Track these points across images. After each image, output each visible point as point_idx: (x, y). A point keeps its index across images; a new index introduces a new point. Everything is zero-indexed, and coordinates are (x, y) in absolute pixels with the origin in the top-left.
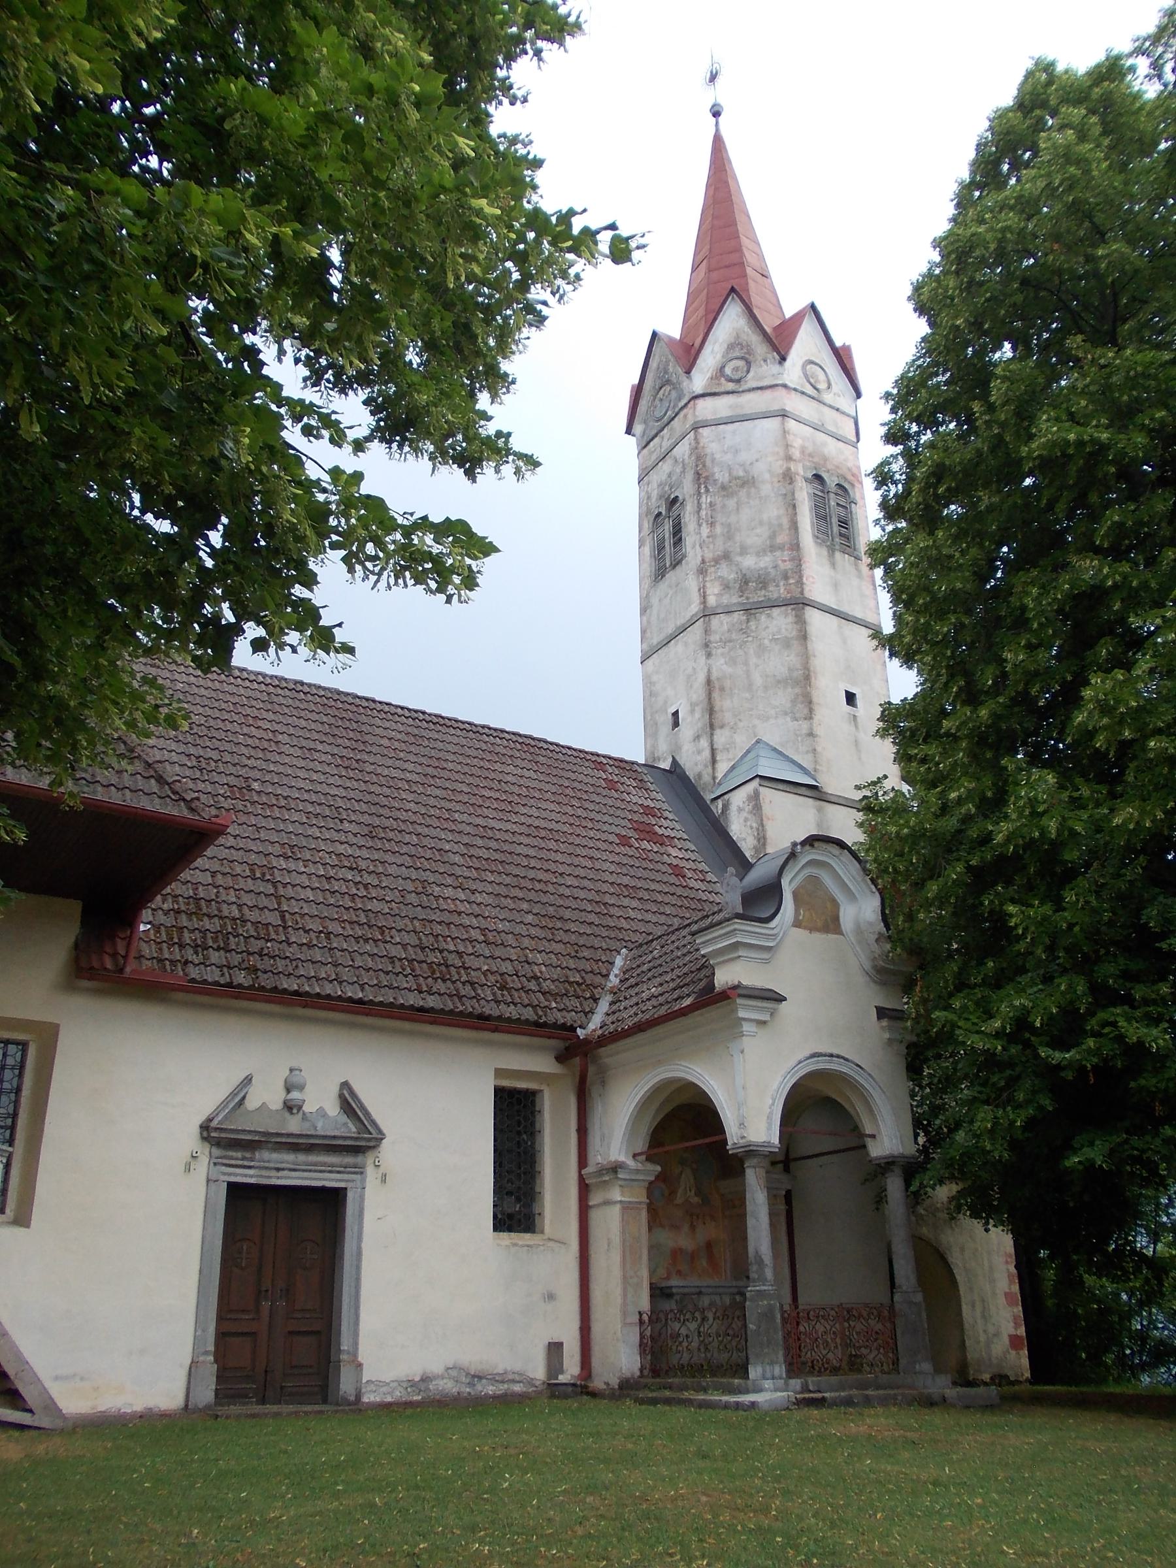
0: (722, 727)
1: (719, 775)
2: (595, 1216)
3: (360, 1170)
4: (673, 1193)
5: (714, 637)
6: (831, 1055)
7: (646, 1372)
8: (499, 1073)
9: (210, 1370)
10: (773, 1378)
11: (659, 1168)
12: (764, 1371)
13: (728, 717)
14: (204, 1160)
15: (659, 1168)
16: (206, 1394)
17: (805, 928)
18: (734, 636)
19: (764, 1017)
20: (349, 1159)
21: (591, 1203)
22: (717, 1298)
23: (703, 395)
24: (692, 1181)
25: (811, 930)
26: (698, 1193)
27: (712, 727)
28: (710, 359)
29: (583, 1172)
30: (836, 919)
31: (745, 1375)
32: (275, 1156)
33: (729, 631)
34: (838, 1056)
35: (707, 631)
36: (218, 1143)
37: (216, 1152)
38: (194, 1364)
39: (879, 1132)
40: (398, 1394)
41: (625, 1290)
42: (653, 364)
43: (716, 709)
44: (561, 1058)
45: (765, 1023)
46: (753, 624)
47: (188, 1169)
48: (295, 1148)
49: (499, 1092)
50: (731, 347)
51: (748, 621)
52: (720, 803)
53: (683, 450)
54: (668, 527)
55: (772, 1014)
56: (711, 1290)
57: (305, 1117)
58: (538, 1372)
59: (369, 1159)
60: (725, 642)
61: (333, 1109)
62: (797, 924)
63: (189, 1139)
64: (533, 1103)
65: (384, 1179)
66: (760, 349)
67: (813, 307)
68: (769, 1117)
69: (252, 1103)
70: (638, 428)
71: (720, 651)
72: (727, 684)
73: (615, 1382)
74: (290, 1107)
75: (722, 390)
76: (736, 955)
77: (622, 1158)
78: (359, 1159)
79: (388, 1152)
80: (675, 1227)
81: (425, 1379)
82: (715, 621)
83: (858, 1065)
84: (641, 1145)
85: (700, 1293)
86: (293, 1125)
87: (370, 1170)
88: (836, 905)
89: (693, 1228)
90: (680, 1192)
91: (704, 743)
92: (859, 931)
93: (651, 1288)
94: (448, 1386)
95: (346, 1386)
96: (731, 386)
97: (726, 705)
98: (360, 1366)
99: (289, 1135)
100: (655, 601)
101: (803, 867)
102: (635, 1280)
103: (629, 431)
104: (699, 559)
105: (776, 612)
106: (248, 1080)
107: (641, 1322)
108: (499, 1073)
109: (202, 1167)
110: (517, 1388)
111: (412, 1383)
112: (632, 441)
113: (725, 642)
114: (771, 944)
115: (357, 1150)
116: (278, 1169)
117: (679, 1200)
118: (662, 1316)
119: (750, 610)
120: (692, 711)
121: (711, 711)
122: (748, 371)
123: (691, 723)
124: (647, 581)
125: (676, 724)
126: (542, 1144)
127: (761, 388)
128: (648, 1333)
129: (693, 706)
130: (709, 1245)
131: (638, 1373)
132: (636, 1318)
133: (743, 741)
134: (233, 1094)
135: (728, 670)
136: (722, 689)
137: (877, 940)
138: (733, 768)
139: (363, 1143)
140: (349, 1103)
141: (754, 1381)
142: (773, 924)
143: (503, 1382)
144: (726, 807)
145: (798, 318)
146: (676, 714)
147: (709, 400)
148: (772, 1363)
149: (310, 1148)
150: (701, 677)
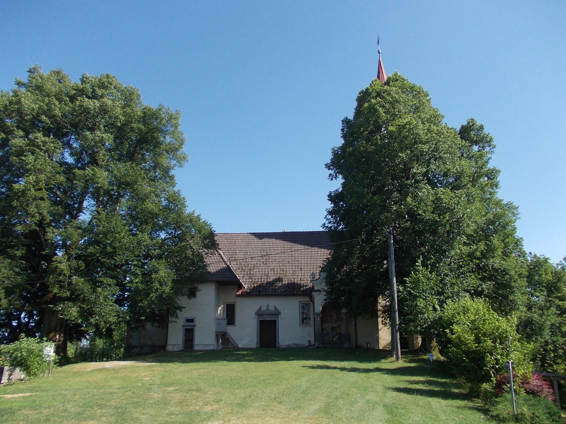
3: (278, 317)
8: (300, 302)
14: (256, 318)
16: (259, 346)
20: (276, 316)
36: (258, 315)
40: (285, 347)
47: (254, 319)
48: (268, 315)
58: (307, 344)
59: (279, 315)
61: (274, 309)
63: (253, 315)
65: (282, 318)
69: (262, 309)
74: (267, 310)
81: (289, 345)
86: (268, 312)
87: (280, 318)
94: (293, 346)
95: (277, 345)
98: (279, 343)
106: (261, 306)
110: (304, 347)
115: (277, 315)
140: (276, 309)
149: (270, 315)
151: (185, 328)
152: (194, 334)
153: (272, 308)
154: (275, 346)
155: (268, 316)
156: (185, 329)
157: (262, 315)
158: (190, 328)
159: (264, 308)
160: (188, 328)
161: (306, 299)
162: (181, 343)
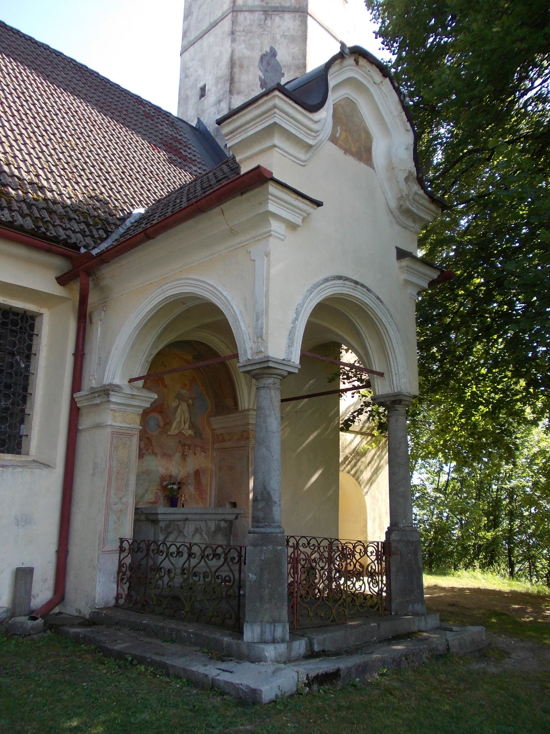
0: (239, 93)
2: (83, 440)
4: (168, 424)
5: (239, 28)
6: (356, 283)
7: (121, 601)
10: (274, 641)
11: (155, 396)
12: (263, 632)
15: (155, 396)
17: (341, 147)
18: (254, 29)
19: (297, 220)
21: (80, 428)
22: (202, 524)
24: (187, 415)
25: (347, 151)
26: (192, 426)
27: (231, 92)
29: (75, 396)
30: (369, 150)
31: (239, 632)
33: (251, 25)
34: (363, 286)
35: (234, 22)
39: (389, 370)
41: (107, 515)
43: (236, 79)
44: (62, 280)
46: (269, 22)
55: (304, 220)
56: (197, 517)
60: (247, 32)
62: (333, 139)
64: (32, 327)
68: (292, 333)
71: (243, 38)
72: (246, 63)
73: (86, 612)
76: (269, 144)
77: (117, 381)
80: (167, 456)
82: (241, 17)
83: (378, 298)
84: (139, 370)
85: (187, 519)
88: (369, 138)
89: (184, 457)
90: (174, 425)
92: (391, 168)
93: (136, 514)
100: (195, 10)
102: (119, 506)
105: (287, 16)
107: (122, 549)
113: (247, 32)
114: (311, 142)
117: (173, 430)
118: (143, 545)
120: (217, 83)
121: (232, 80)
126: (36, 368)
128: (128, 561)
129: (217, 80)
130: (197, 473)
131: (114, 602)
132: (116, 545)
135: (247, 53)
136: (241, 66)
137: (407, 179)
141: (249, 644)
146: (203, 89)
148: (274, 622)
150: (226, 58)
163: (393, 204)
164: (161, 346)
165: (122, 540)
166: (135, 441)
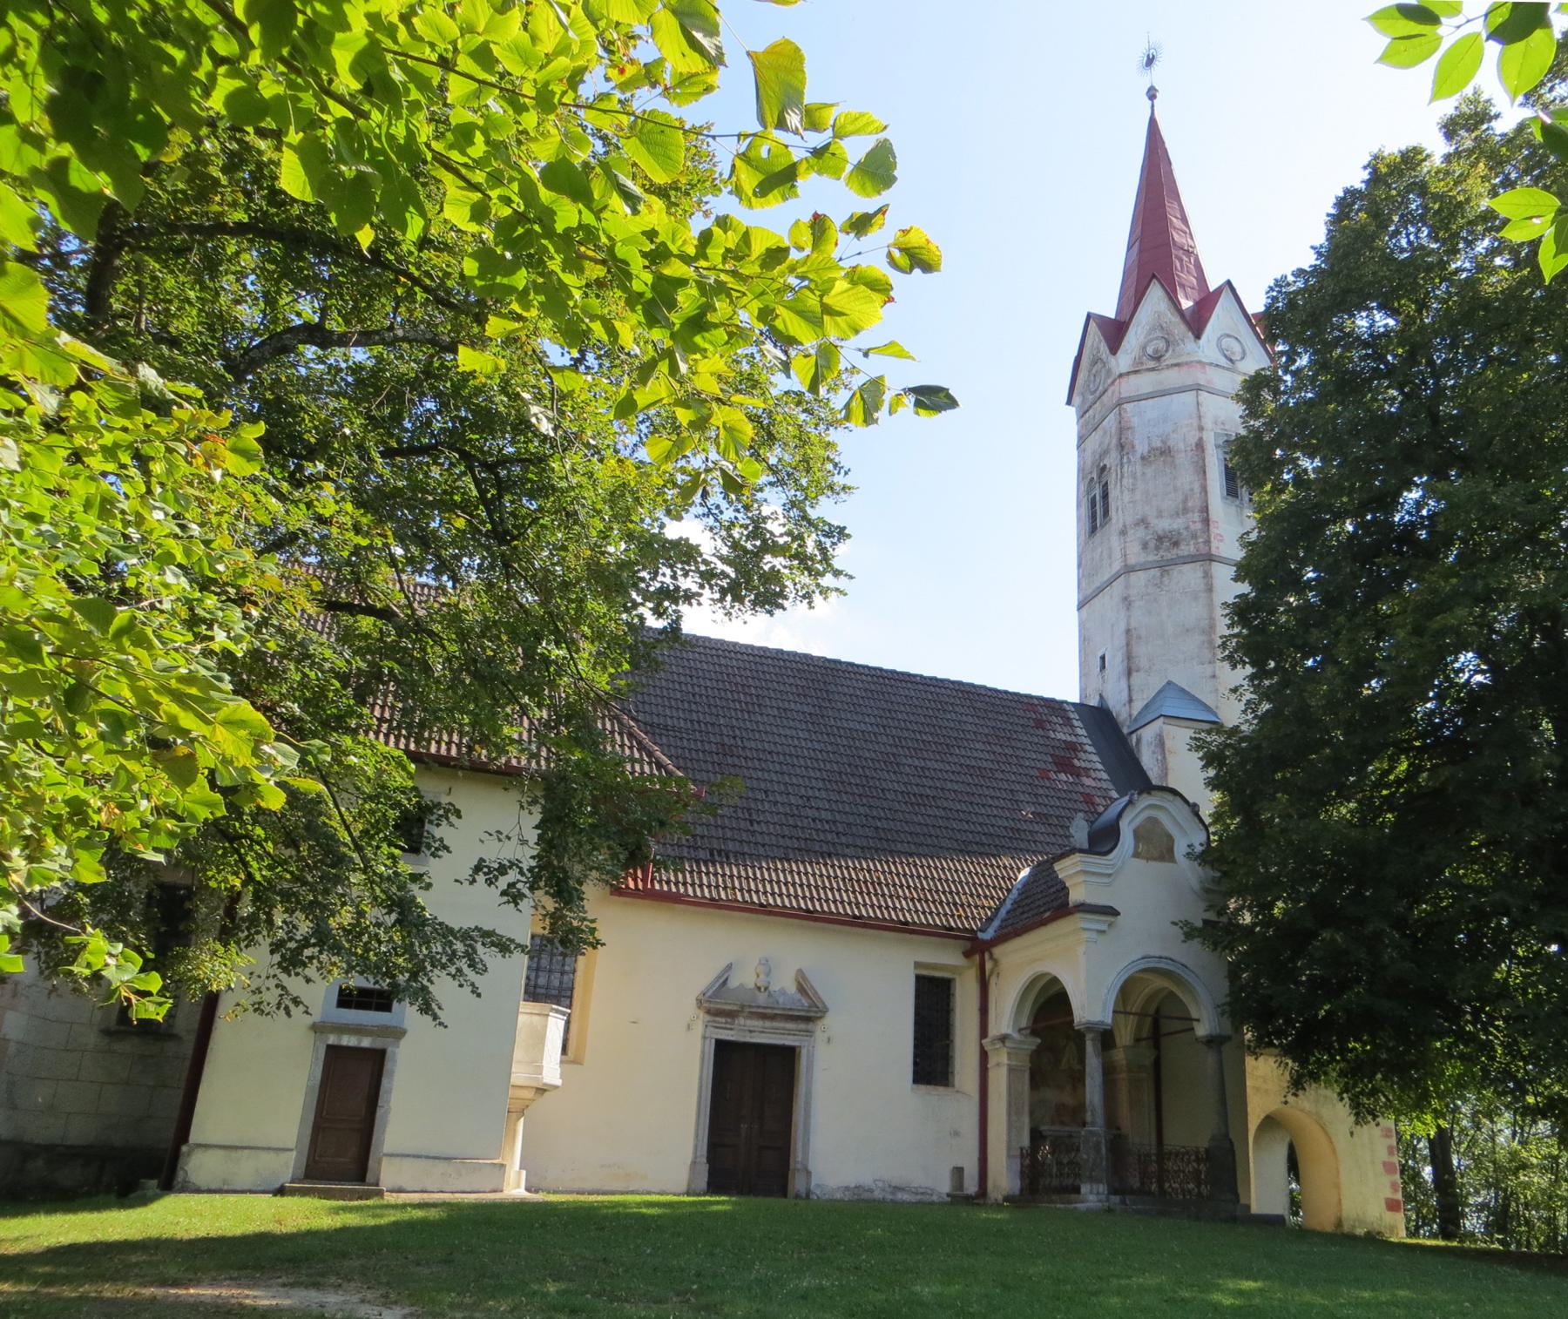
0: (1138, 671)
1: (1135, 713)
3: (810, 1033)
8: (917, 965)
9: (704, 1168)
11: (1039, 1041)
13: (1143, 662)
15: (1039, 1041)
17: (1143, 858)
19: (1104, 927)
20: (802, 1026)
23: (1128, 373)
28: (1133, 339)
30: (1171, 850)
32: (749, 1022)
36: (709, 1012)
37: (708, 1018)
38: (694, 1163)
42: (1088, 342)
44: (967, 954)
45: (1103, 932)
48: (764, 1016)
49: (919, 979)
50: (1153, 329)
51: (1162, 576)
52: (1134, 736)
53: (1110, 422)
54: (1098, 492)
57: (770, 995)
58: (945, 1186)
59: (819, 1027)
61: (791, 988)
62: (1136, 855)
63: (689, 1008)
66: (1179, 329)
67: (1229, 283)
69: (733, 983)
70: (1077, 399)
75: (1144, 367)
78: (810, 1026)
79: (828, 1020)
84: (1024, 1023)
86: (762, 999)
87: (818, 1034)
88: (1171, 839)
90: (1065, 1060)
91: (1124, 684)
95: (797, 1184)
96: (1152, 364)
97: (1141, 651)
98: (809, 1173)
99: (759, 1007)
101: (1146, 808)
103: (1069, 402)
104: (1121, 525)
106: (729, 967)
107: (1022, 1156)
108: (917, 965)
109: (699, 1028)
111: (847, 1188)
112: (1072, 412)
115: (808, 1019)
116: (751, 1031)
117: (1064, 1065)
119: (1164, 566)
122: (1167, 351)
123: (1116, 664)
124: (1083, 538)
125: (1103, 667)
127: (1177, 365)
132: (1018, 1153)
133: (1157, 684)
134: (719, 977)
138: (1147, 706)
139: (812, 1014)
142: (1111, 856)
143: (917, 1194)
144: (1139, 741)
145: (1219, 291)
146: (1103, 658)
147: (1132, 377)
149: (773, 1017)
150: (1122, 626)
151: (332, 1039)
152: (385, 1081)
153: (784, 983)
154: (783, 1191)
155: (757, 1024)
156: (330, 1048)
157: (731, 1015)
158: (366, 1043)
159: (744, 978)
160: (348, 1041)
161: (944, 958)
162: (291, 1141)
163: (1196, 886)
164: (1042, 1000)
165: (1022, 1149)
166: (1027, 1076)
